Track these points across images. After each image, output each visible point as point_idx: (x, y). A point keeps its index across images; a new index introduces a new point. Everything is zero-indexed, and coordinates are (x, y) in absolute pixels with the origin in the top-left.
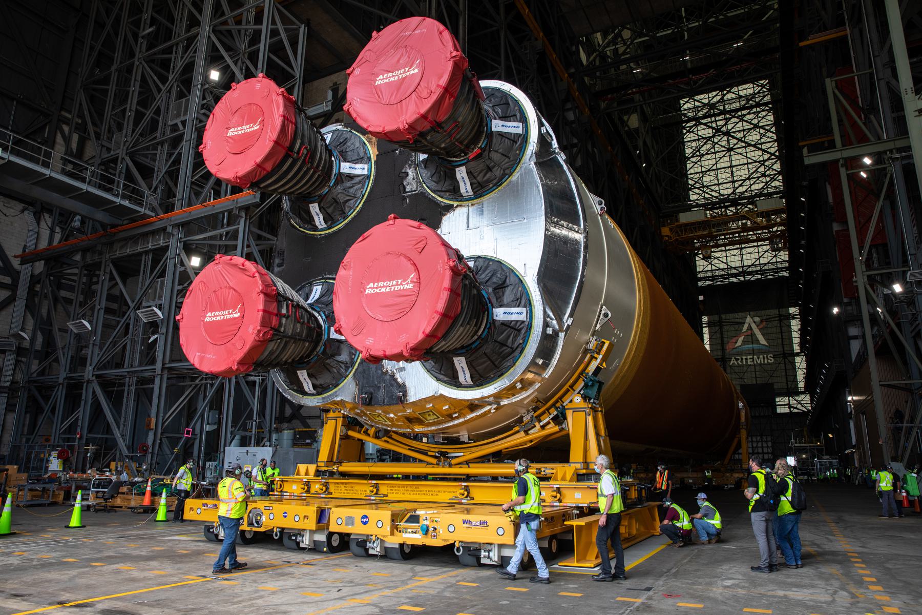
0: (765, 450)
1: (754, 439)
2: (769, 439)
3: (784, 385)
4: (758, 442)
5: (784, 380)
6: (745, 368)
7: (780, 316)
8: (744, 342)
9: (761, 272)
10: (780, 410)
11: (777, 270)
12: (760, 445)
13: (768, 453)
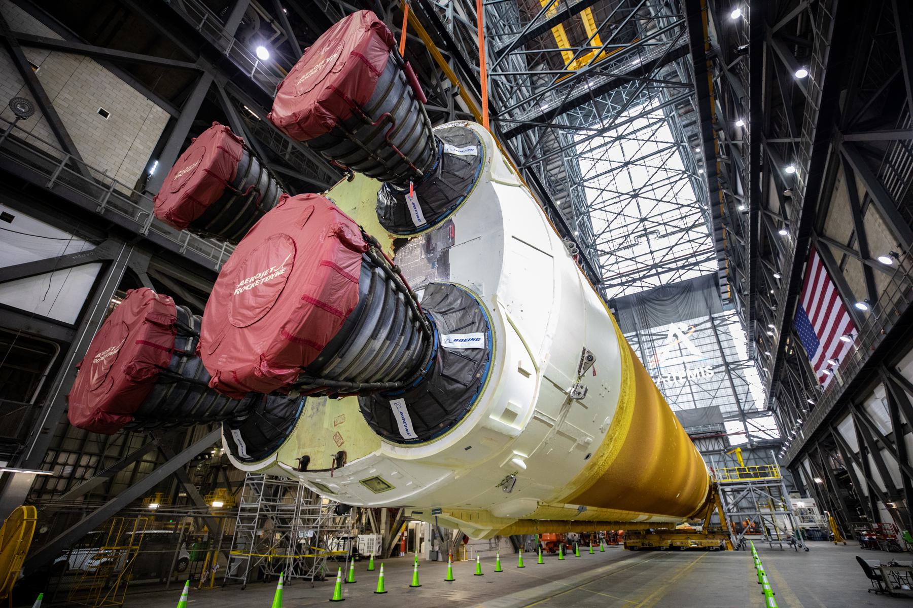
6: (678, 390)
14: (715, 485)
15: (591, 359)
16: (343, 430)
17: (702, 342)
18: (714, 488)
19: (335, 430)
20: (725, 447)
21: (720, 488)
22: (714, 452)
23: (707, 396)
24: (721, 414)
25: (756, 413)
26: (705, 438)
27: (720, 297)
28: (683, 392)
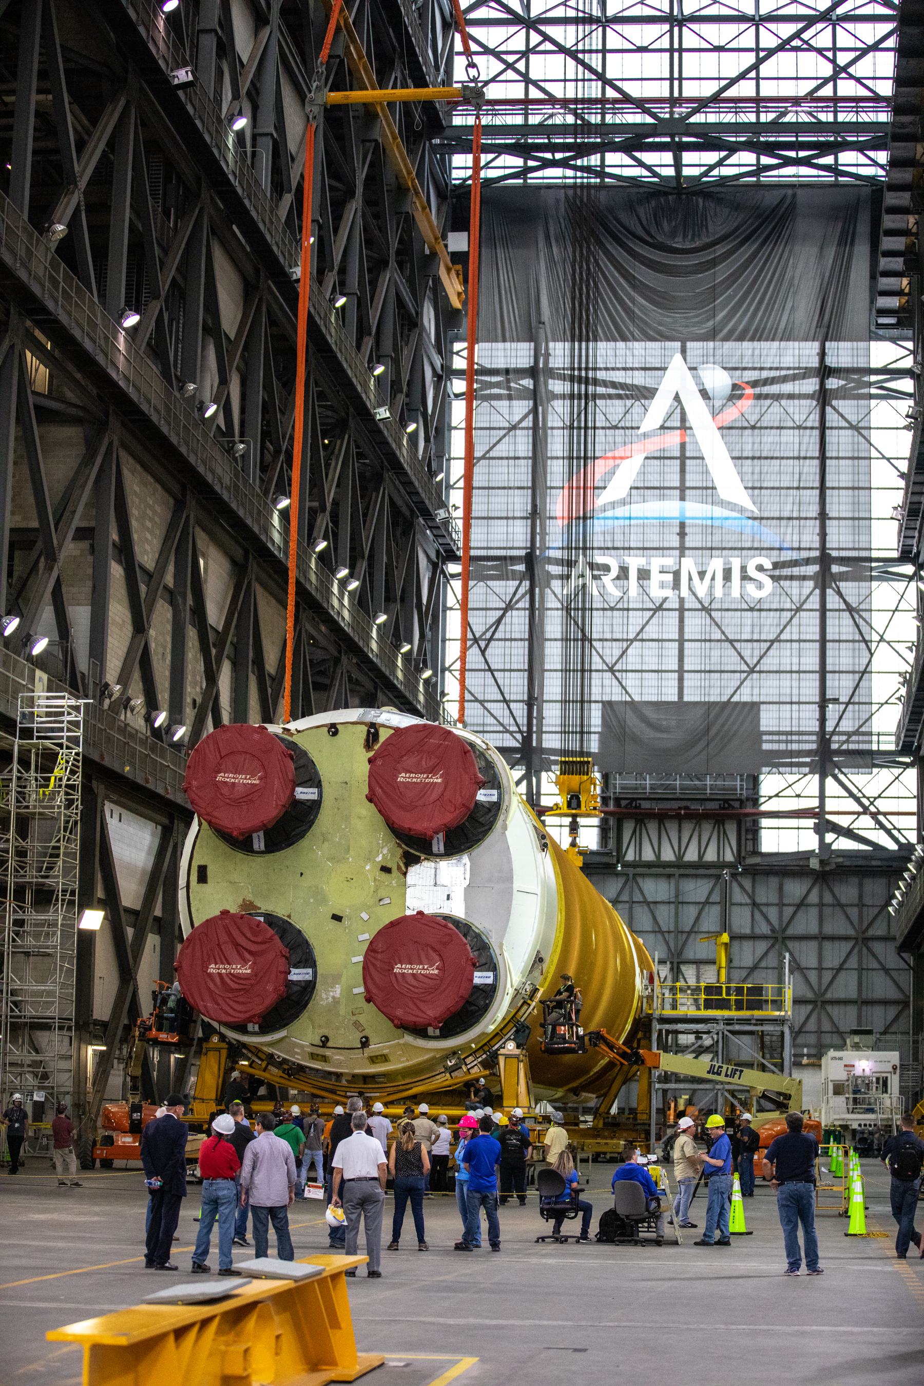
3: (808, 719)
5: (810, 688)
6: (636, 620)
7: (825, 371)
9: (757, 139)
10: (780, 839)
11: (834, 139)
14: (649, 1017)
15: (541, 960)
16: (362, 1019)
17: (768, 441)
18: (643, 1025)
19: (354, 1018)
20: (740, 858)
21: (656, 1026)
22: (700, 869)
23: (731, 660)
24: (757, 736)
25: (868, 759)
26: (681, 817)
27: (873, 277)
28: (651, 631)
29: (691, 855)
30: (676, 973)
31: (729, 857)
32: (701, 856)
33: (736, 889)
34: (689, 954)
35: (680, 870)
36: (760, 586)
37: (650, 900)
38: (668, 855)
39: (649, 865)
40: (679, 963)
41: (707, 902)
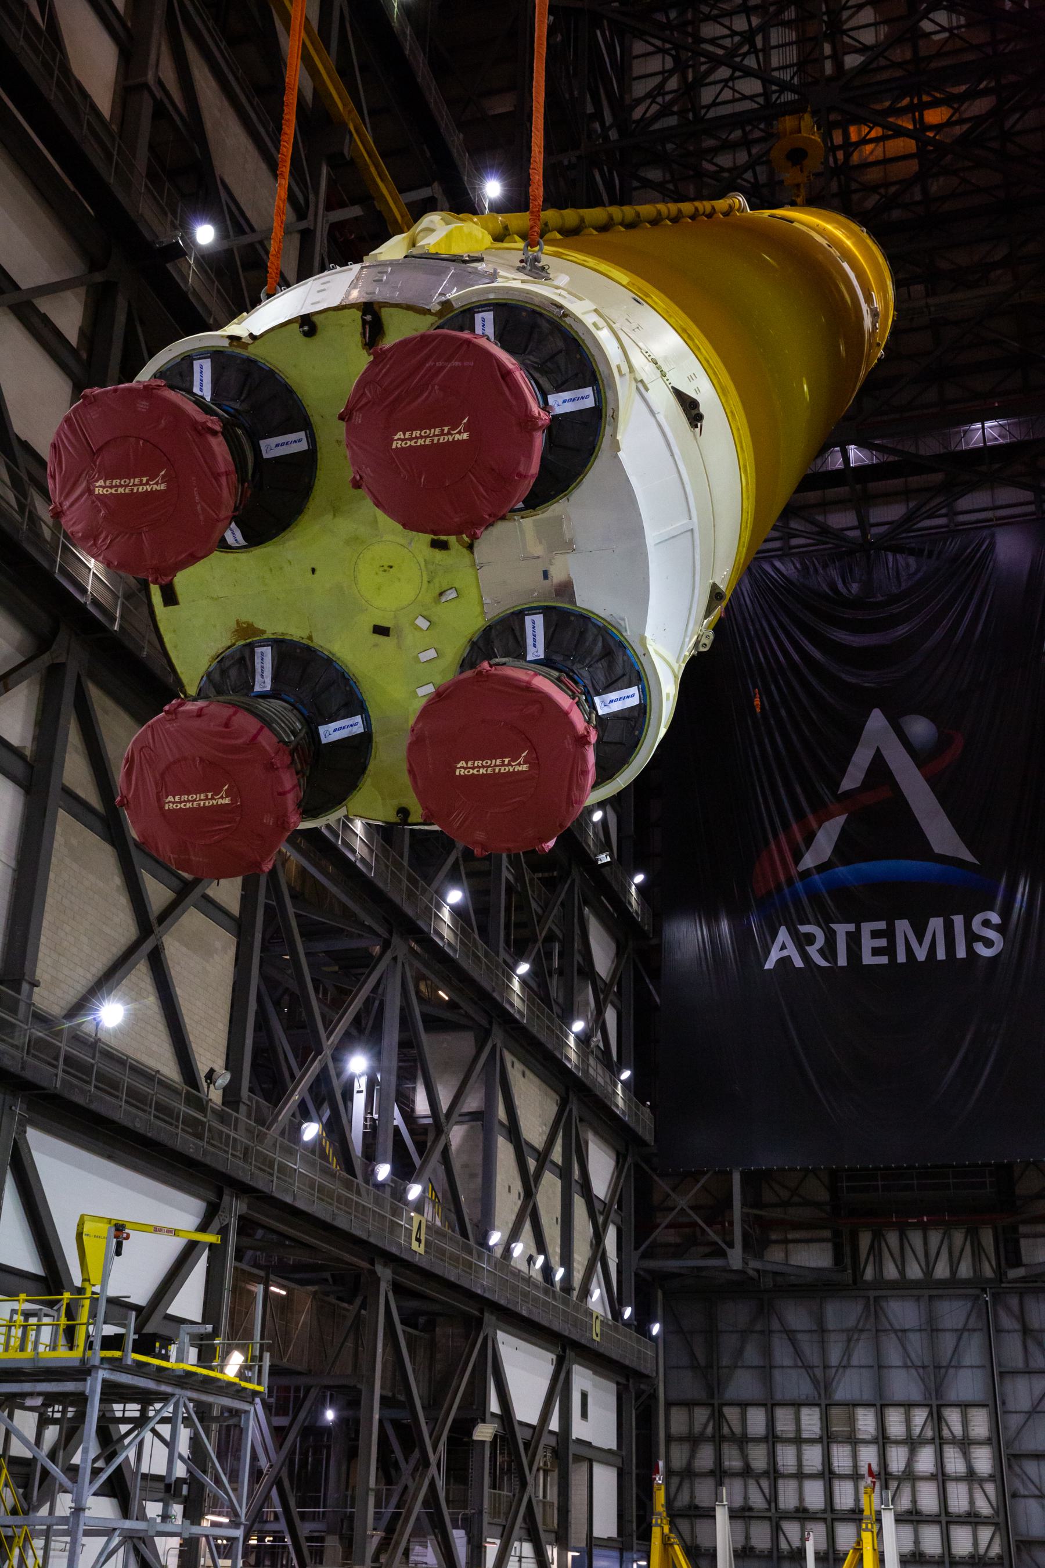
0: (959, 1499)
1: (895, 1425)
2: (980, 1425)
4: (912, 1443)
8: (846, 849)
12: (926, 1461)
13: (972, 1519)
29: (942, 1271)
30: (937, 1418)
31: (988, 1272)
32: (954, 1271)
33: (1002, 1314)
34: (952, 1396)
35: (929, 1290)
36: (989, 943)
37: (898, 1327)
38: (914, 1272)
39: (893, 1285)
40: (939, 1406)
41: (964, 1329)
